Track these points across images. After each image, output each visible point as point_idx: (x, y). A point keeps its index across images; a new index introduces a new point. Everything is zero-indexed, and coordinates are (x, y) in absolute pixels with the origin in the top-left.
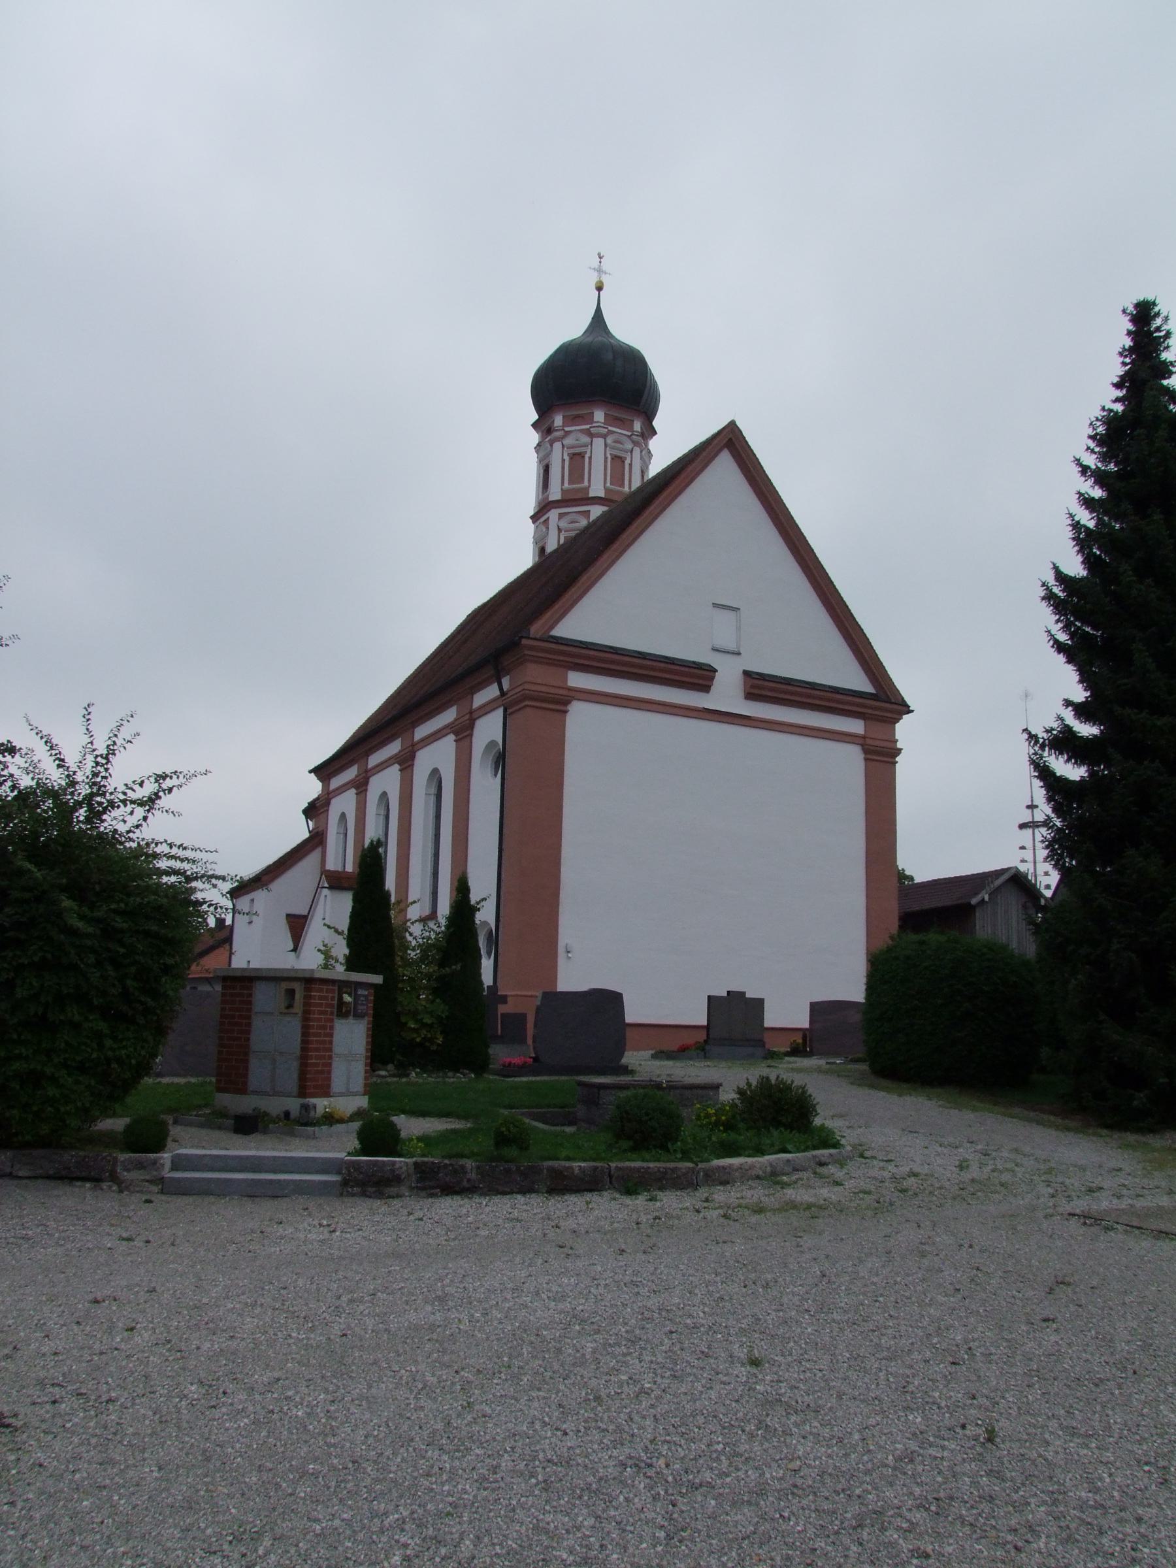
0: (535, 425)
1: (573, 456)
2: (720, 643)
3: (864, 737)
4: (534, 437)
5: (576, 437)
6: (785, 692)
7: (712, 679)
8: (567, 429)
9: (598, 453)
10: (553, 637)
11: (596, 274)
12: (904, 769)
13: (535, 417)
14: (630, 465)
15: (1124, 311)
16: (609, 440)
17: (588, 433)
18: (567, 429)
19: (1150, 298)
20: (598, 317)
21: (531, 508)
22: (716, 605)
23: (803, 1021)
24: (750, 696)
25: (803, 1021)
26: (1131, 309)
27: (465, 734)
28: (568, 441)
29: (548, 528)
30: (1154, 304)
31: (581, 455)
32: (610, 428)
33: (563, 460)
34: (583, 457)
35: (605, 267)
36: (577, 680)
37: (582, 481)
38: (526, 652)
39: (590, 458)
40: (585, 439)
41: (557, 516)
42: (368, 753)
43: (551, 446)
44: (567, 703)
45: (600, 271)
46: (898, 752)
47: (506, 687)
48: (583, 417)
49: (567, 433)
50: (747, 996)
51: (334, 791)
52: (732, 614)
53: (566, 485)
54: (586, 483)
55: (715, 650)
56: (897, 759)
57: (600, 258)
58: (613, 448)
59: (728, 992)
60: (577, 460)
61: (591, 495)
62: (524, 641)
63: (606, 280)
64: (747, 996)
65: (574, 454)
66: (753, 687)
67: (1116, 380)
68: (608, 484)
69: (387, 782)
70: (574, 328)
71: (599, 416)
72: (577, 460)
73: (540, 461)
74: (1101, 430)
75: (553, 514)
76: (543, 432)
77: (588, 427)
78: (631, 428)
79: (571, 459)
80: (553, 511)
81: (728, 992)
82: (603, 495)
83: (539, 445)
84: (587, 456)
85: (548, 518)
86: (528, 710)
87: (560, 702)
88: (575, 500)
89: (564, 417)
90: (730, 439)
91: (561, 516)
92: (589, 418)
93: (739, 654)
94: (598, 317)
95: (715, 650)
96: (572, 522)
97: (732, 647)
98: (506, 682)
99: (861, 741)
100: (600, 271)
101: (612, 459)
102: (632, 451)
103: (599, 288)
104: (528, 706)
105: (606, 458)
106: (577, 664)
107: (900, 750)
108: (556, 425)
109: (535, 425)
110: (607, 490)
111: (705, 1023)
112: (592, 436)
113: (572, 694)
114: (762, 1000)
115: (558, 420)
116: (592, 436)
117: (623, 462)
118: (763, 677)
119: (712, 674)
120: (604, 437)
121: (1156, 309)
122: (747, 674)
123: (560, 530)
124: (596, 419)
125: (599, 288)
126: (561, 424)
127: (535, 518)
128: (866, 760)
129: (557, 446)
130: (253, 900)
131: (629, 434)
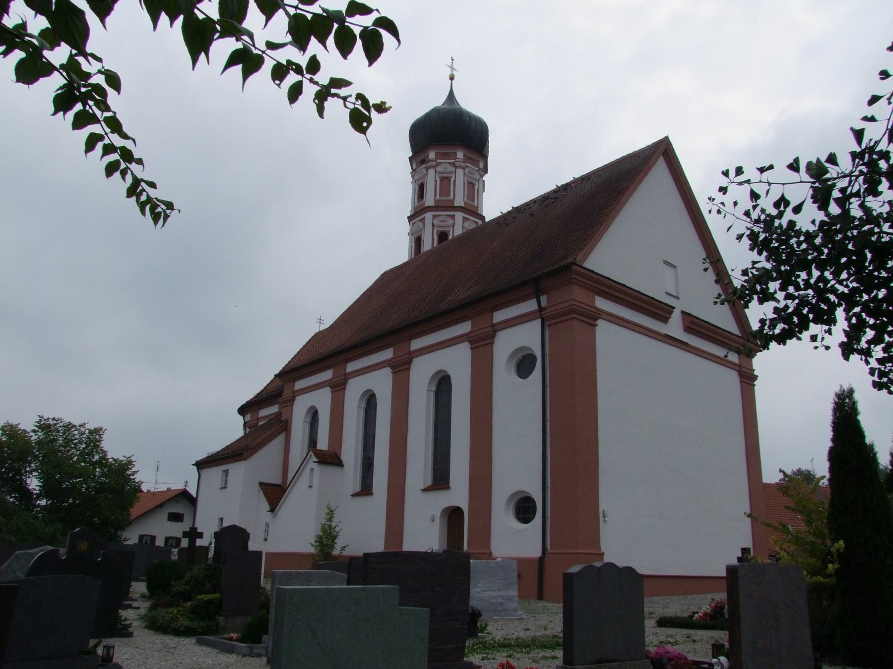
1: (442, 179)
3: (740, 366)
5: (445, 166)
8: (438, 161)
9: (460, 178)
11: (450, 70)
12: (760, 389)
13: (411, 154)
14: (478, 189)
16: (467, 171)
17: (453, 164)
18: (438, 161)
20: (451, 96)
21: (408, 211)
27: (488, 341)
28: (439, 169)
29: (424, 224)
31: (449, 179)
33: (436, 181)
34: (450, 180)
35: (455, 67)
36: (602, 303)
37: (449, 195)
38: (574, 276)
39: (455, 181)
40: (452, 169)
41: (432, 216)
43: (427, 171)
44: (596, 319)
45: (452, 68)
46: (755, 378)
47: (544, 303)
48: (449, 155)
49: (438, 164)
51: (298, 391)
53: (438, 197)
54: (452, 197)
56: (755, 383)
57: (453, 60)
58: (467, 176)
60: (445, 182)
61: (456, 204)
62: (574, 267)
63: (455, 73)
65: (444, 178)
68: (466, 199)
70: (438, 101)
71: (460, 155)
72: (445, 182)
73: (415, 181)
75: (429, 216)
77: (453, 161)
78: (478, 166)
79: (441, 180)
80: (428, 213)
82: (463, 205)
84: (452, 179)
85: (425, 217)
86: (575, 320)
87: (592, 317)
88: (443, 207)
89: (436, 153)
91: (434, 217)
94: (451, 96)
96: (442, 222)
99: (737, 368)
100: (452, 68)
101: (468, 184)
103: (452, 78)
104: (574, 318)
105: (464, 183)
106: (602, 291)
107: (757, 376)
110: (465, 203)
112: (456, 167)
116: (456, 167)
117: (474, 187)
119: (671, 309)
120: (464, 169)
123: (433, 226)
125: (452, 78)
126: (434, 157)
127: (410, 218)
128: (741, 381)
129: (431, 172)
130: (226, 472)
131: (477, 169)
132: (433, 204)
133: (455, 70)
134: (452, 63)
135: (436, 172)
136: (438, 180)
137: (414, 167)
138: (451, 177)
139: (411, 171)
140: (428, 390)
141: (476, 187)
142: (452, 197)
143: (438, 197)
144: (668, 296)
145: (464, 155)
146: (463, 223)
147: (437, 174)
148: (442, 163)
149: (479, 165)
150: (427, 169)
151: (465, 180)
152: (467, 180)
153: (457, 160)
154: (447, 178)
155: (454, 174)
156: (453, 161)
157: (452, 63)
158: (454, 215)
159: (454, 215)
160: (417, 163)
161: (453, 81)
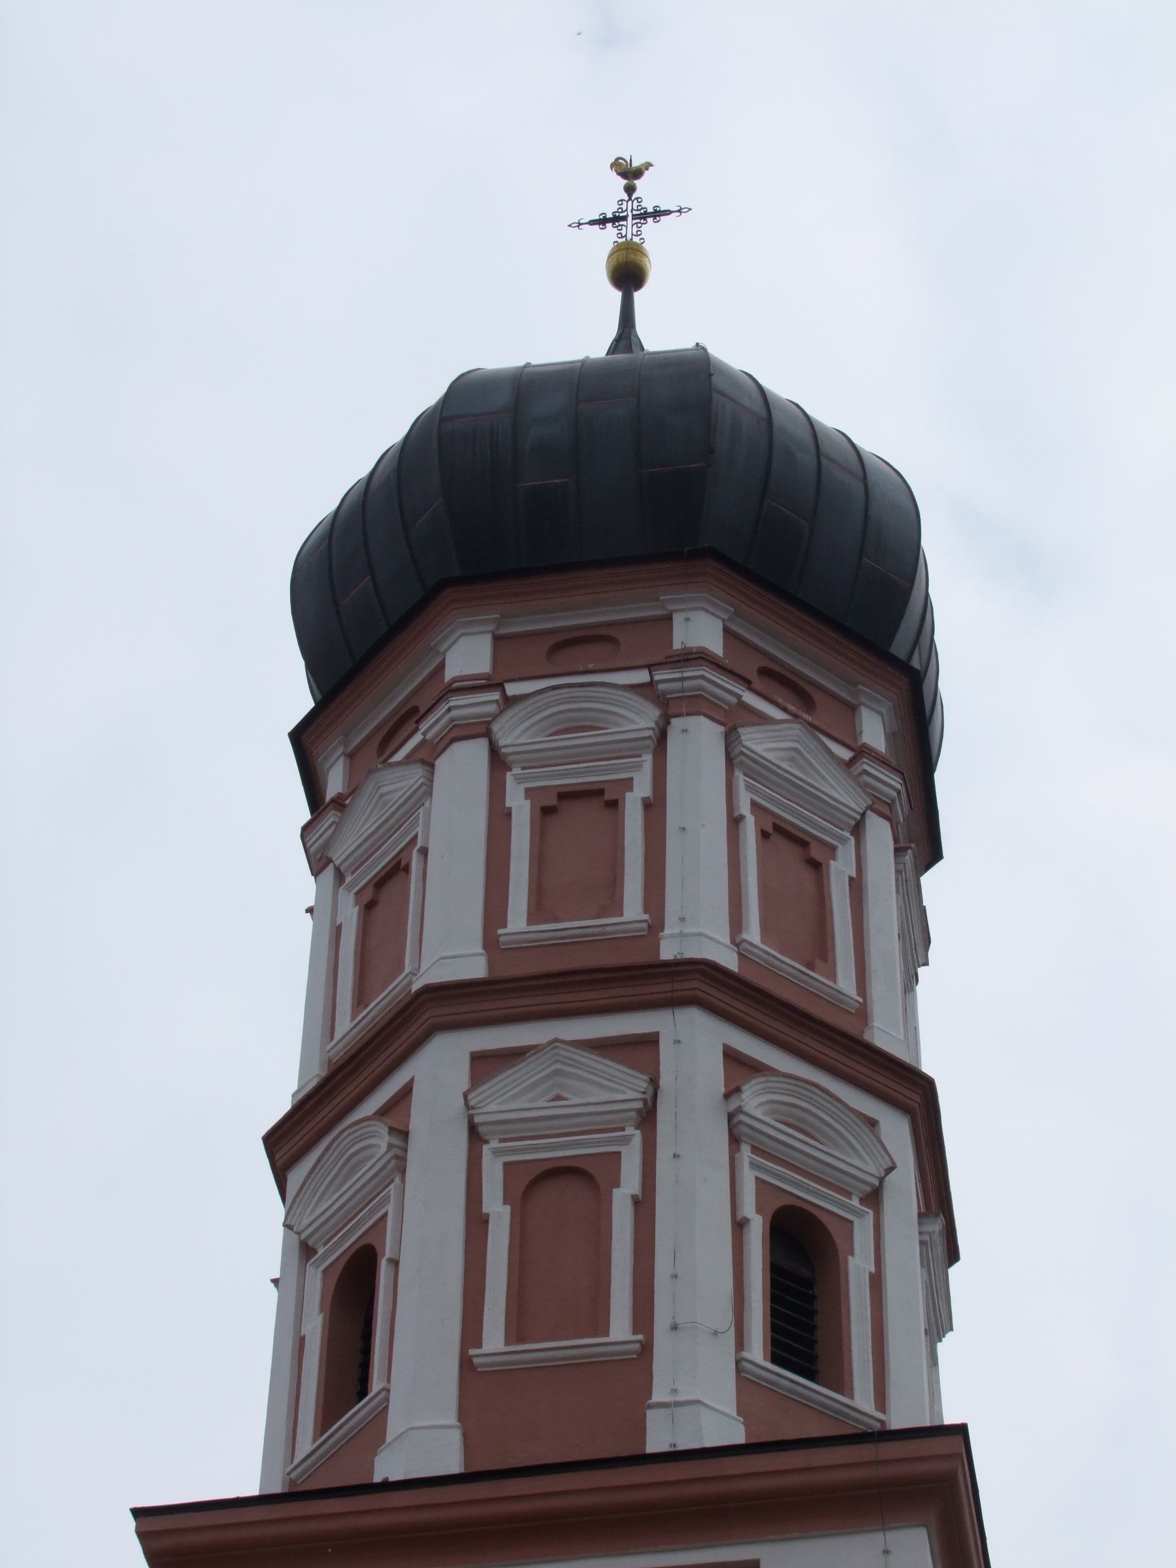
8: (512, 689)
18: (512, 689)
29: (404, 1134)
34: (614, 805)
65: (568, 795)
89: (497, 639)
101: (764, 835)
102: (858, 829)
105: (735, 821)
117: (816, 866)
131: (846, 755)
132: (476, 968)
135: (495, 754)
137: (335, 784)
138: (628, 784)
139: (306, 816)
141: (840, 869)
142: (633, 910)
143: (517, 920)
145: (727, 631)
146: (732, 1092)
149: (855, 732)
150: (427, 758)
151: (745, 809)
152: (755, 805)
154: (592, 793)
155: (648, 759)
158: (650, 1041)
159: (650, 1041)
160: (351, 756)
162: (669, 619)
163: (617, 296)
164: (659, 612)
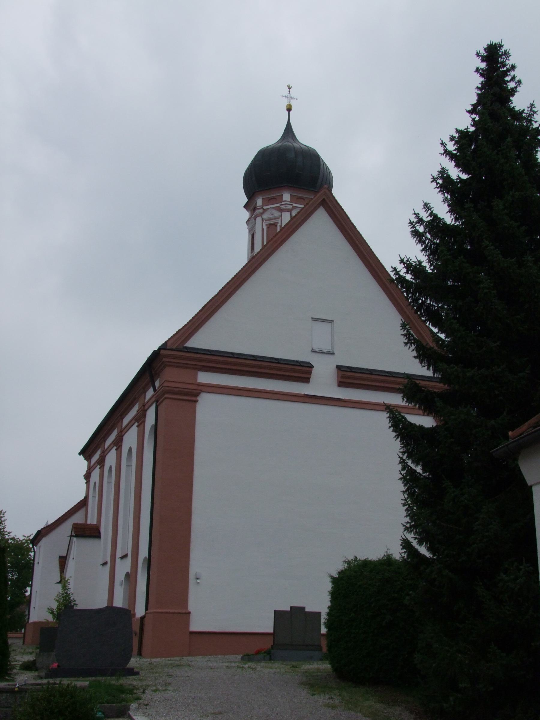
0: (246, 206)
2: (317, 347)
4: (246, 215)
5: (271, 213)
6: (368, 380)
7: (310, 373)
8: (265, 208)
10: (186, 348)
15: (478, 55)
18: (265, 208)
19: (496, 41)
20: (289, 130)
22: (314, 319)
23: (268, 627)
24: (342, 384)
25: (268, 627)
26: (483, 52)
28: (266, 216)
30: (501, 46)
32: (294, 205)
33: (263, 230)
34: (276, 226)
36: (204, 378)
38: (164, 359)
40: (277, 214)
42: (105, 439)
43: (255, 220)
44: (197, 395)
48: (276, 199)
49: (265, 210)
50: (307, 610)
52: (327, 326)
55: (314, 351)
57: (289, 88)
59: (291, 607)
63: (293, 103)
64: (307, 610)
66: (342, 377)
67: (470, 108)
69: (111, 459)
71: (286, 197)
73: (250, 231)
74: (451, 147)
76: (251, 211)
77: (278, 205)
79: (268, 228)
81: (291, 607)
83: (248, 220)
89: (263, 199)
90: (324, 199)
92: (279, 199)
93: (333, 354)
94: (289, 130)
95: (314, 351)
97: (328, 348)
98: (157, 384)
100: (289, 97)
103: (289, 109)
106: (204, 366)
108: (258, 205)
109: (246, 206)
111: (271, 630)
112: (281, 211)
113: (200, 388)
114: (276, 612)
115: (259, 202)
116: (281, 211)
118: (351, 369)
120: (290, 211)
121: (503, 50)
122: (339, 368)
124: (284, 199)
125: (289, 109)
129: (259, 219)
133: (293, 99)
134: (289, 91)
135: (263, 220)
136: (265, 227)
140: (126, 466)
144: (314, 354)
147: (264, 221)
148: (268, 209)
153: (283, 203)
155: (280, 218)
156: (278, 205)
157: (289, 91)
161: (290, 112)
162: (282, 195)
163: (288, 112)
164: (281, 194)
